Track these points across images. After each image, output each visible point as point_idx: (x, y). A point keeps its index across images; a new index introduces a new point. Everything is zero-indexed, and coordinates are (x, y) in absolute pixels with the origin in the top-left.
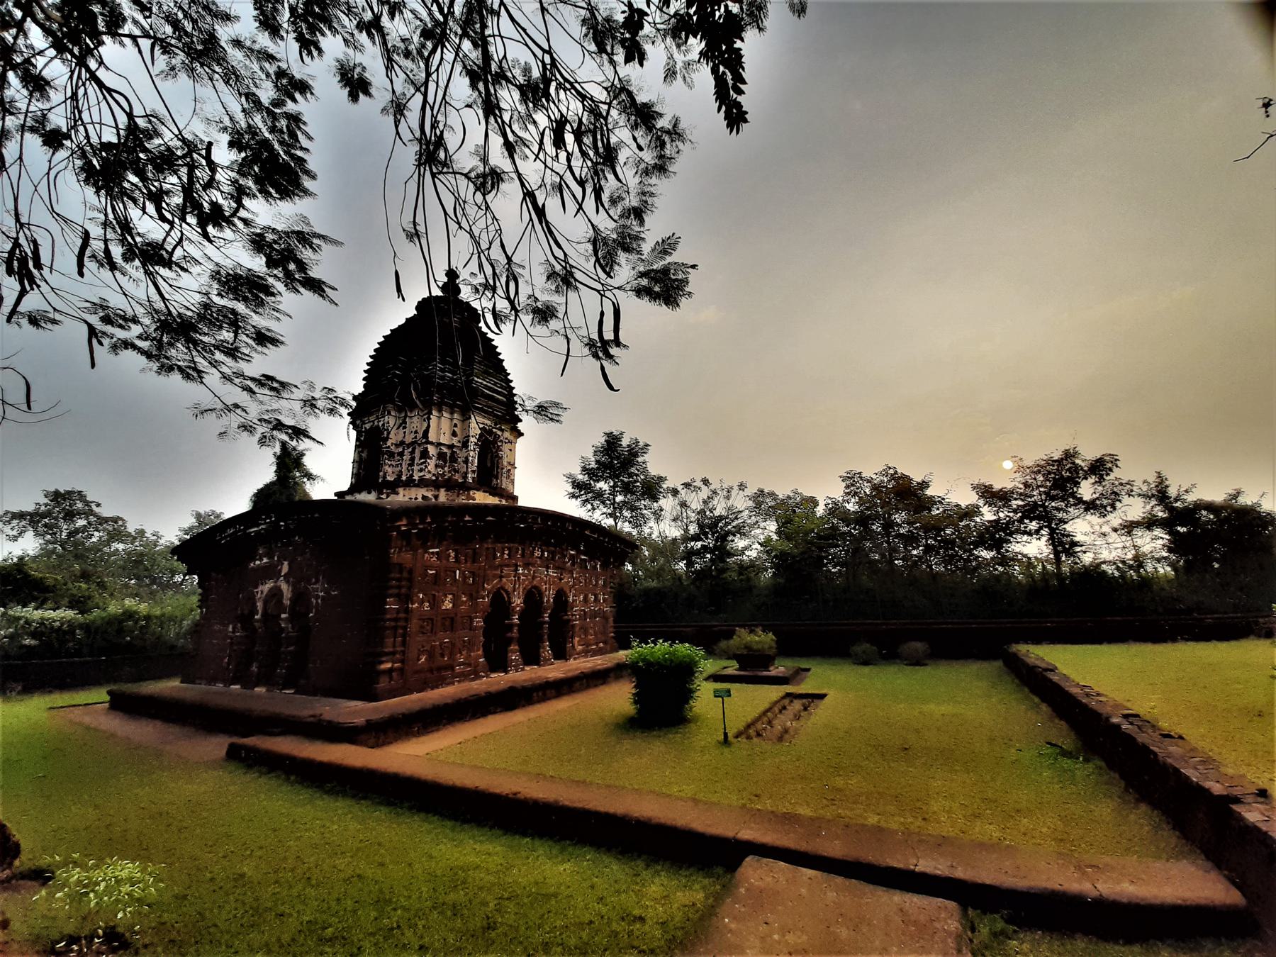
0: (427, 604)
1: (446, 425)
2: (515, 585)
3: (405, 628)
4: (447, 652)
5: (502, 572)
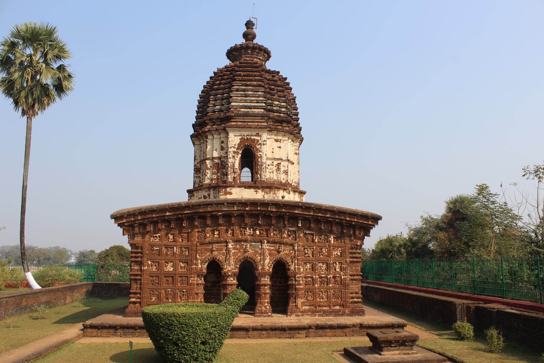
0: (155, 267)
1: (217, 144)
2: (226, 257)
3: (141, 280)
4: (170, 296)
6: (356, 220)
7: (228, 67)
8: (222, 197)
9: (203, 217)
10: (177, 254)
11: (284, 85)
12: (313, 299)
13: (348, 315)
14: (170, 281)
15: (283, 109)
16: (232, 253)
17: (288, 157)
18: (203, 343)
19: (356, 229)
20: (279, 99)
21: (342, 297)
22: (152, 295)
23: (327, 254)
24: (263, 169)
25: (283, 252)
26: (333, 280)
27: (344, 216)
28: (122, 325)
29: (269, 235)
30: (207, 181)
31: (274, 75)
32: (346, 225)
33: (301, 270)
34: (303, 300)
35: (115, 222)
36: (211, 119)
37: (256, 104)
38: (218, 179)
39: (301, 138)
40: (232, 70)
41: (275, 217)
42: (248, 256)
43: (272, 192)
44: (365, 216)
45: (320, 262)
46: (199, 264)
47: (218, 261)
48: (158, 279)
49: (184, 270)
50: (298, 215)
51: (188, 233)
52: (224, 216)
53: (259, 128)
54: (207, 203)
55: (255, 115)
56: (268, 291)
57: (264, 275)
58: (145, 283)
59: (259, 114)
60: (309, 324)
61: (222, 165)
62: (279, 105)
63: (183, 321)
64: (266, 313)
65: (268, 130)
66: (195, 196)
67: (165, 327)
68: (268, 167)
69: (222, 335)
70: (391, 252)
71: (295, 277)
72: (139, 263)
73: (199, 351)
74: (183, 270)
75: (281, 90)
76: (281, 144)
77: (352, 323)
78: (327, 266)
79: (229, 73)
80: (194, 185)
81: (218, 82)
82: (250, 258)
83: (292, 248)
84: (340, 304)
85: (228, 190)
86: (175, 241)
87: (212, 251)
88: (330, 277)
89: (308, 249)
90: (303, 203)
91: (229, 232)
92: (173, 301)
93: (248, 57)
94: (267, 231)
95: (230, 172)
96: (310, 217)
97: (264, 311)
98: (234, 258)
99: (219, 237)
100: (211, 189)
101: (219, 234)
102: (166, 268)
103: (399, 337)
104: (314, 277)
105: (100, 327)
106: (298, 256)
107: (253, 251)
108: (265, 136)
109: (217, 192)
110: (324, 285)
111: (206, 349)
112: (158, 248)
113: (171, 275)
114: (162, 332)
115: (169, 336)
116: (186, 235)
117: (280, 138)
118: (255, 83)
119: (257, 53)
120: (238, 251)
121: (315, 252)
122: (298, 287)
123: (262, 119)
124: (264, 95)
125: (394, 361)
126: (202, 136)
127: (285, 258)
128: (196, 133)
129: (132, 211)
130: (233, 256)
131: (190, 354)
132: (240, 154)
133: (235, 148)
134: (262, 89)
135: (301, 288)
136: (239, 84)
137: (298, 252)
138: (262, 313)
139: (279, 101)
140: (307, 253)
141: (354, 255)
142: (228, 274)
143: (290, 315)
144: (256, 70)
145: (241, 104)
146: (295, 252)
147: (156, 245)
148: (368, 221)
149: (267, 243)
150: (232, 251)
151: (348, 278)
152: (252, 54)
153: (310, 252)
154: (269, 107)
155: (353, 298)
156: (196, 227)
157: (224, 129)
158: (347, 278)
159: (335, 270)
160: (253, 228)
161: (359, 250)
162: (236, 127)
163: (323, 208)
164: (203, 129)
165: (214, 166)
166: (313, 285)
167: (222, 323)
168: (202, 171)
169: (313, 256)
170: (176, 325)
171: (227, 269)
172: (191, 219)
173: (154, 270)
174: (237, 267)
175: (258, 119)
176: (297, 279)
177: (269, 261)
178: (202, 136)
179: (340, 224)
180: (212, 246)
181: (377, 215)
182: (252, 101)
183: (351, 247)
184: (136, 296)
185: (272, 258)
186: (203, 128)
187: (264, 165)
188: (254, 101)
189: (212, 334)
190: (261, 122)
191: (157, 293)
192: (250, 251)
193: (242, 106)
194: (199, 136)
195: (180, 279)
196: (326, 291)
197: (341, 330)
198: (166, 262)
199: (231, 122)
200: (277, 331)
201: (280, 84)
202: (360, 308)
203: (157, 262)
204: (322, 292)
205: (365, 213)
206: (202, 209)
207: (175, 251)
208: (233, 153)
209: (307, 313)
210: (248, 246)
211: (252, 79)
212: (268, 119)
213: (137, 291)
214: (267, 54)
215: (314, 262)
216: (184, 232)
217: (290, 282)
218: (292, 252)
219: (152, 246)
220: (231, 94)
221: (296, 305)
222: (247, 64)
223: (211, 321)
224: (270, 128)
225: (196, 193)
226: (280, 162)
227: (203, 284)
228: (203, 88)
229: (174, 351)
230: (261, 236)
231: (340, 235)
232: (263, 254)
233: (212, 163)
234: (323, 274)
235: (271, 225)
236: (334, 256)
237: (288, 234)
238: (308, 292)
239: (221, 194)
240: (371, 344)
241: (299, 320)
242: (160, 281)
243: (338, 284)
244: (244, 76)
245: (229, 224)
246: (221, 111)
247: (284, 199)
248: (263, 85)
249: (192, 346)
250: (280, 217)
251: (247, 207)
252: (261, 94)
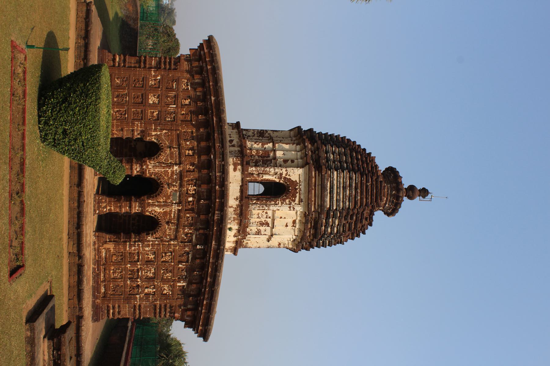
0: (153, 83)
1: (292, 155)
2: (164, 163)
3: (140, 67)
5: (174, 148)
6: (203, 311)
7: (376, 169)
8: (231, 160)
9: (209, 137)
10: (168, 108)
11: (356, 231)
12: (113, 262)
13: (94, 302)
14: (137, 100)
15: (329, 230)
16: (168, 169)
17: (275, 234)
18: (65, 132)
19: (193, 312)
20: (341, 224)
21: (114, 295)
22: (122, 79)
23: (165, 278)
24: (262, 207)
25: (168, 228)
26: (135, 285)
27: (208, 298)
28: (89, 44)
29: (187, 212)
30: (249, 144)
31: (368, 220)
32: (197, 300)
33: (147, 248)
34: (112, 250)
35: (205, 40)
36: (318, 149)
37: (335, 199)
38: (251, 156)
39: (298, 250)
40: (373, 173)
41: (208, 219)
42: (164, 188)
43: (236, 216)
44: (208, 322)
45: (156, 270)
46: (156, 133)
47: (158, 153)
48: (140, 87)
49: (150, 116)
50: (209, 245)
51: (191, 121)
52: (210, 161)
53: (308, 203)
54: (224, 142)
55: (322, 198)
56: (123, 210)
57: (142, 206)
58: (136, 72)
59: (324, 203)
60: (84, 256)
61: (267, 161)
62: (335, 225)
63: (90, 109)
64: (98, 208)
65: (306, 213)
66: (232, 131)
67: (84, 88)
68: (264, 212)
69: (74, 154)
70: (167, 356)
71: (138, 241)
72: (159, 66)
73: (56, 127)
74: (149, 114)
75: (351, 227)
76: (290, 227)
77: (84, 307)
78: (151, 278)
79: (370, 169)
80: (245, 130)
81: (359, 157)
82: (162, 190)
83: (172, 238)
84: (107, 293)
85: (239, 167)
86: (183, 106)
87: (170, 147)
88: (138, 282)
89: (170, 257)
90: (223, 250)
91: (191, 167)
92: (115, 103)
93: (388, 191)
94: (192, 210)
95: (259, 169)
96: (207, 259)
98: (162, 172)
99: (186, 155)
100: (240, 148)
101: (189, 155)
102: (152, 96)
103: (65, 359)
104: (138, 263)
105: (87, 20)
106: (162, 245)
107: (169, 194)
108: (299, 209)
109: (237, 155)
110: (130, 274)
111: (58, 135)
112: (174, 87)
113: (144, 101)
114: (78, 85)
115: (74, 93)
116: (189, 119)
117: (297, 226)
118: (359, 198)
119: (393, 201)
120: (169, 176)
121: (167, 264)
122: (128, 245)
123: (318, 206)
124: (345, 208)
125: (36, 354)
126: (300, 138)
127: (160, 230)
128: (303, 132)
129: (216, 59)
130: (164, 171)
131: (52, 116)
132: (280, 181)
133: (286, 175)
134: (352, 205)
135: (126, 248)
136: (357, 180)
137: (168, 244)
138: (98, 203)
139: (338, 225)
140: (166, 255)
141: (163, 310)
142: (144, 165)
143: (95, 235)
144: (373, 199)
145: (335, 182)
146: (168, 241)
147: (178, 85)
148: (202, 326)
149: (179, 210)
150: (170, 170)
151: (137, 302)
152: (391, 195)
153: (167, 258)
154: (332, 213)
155: (114, 308)
156: (198, 130)
157: (307, 163)
158: (137, 301)
159: (146, 288)
160: (195, 193)
161: (169, 315)
162: (309, 177)
163: (217, 274)
164: (307, 140)
165: (266, 151)
166: (129, 262)
167: (87, 153)
168: (261, 138)
169: (163, 262)
170: (86, 100)
171: (149, 164)
172: (207, 124)
173: (150, 83)
174: (151, 175)
175: (318, 201)
176: (137, 243)
177: (157, 212)
178: (300, 138)
179: (199, 293)
180: (176, 148)
181: (209, 336)
182: (339, 195)
183: (173, 306)
184: (122, 62)
185: (161, 215)
186: (309, 141)
187: (267, 208)
188: (339, 197)
189: (75, 141)
190: (315, 204)
191: (124, 85)
192: (170, 191)
193: (333, 183)
194: (299, 136)
195: (140, 112)
196: (122, 277)
197: (76, 293)
198: (159, 96)
199: (315, 171)
200: (77, 219)
201: (358, 227)
202: (102, 317)
203: (159, 86)
204: (121, 272)
205: (212, 321)
206: (218, 136)
207: (171, 106)
208: (280, 173)
209: (98, 254)
210: (175, 189)
211: (363, 195)
212: (318, 212)
213: (127, 63)
214: (391, 212)
215: (156, 263)
216: (193, 116)
217: (133, 236)
218: (168, 237)
219: (178, 81)
220: (347, 171)
221: (106, 242)
222: (380, 189)
223: (89, 140)
224: (309, 215)
225: (236, 132)
226: (270, 225)
227: (133, 136)
228: (352, 140)
229: (57, 98)
230: (186, 203)
231: (187, 293)
232: (166, 204)
233: (269, 149)
234: (142, 273)
235: (199, 214)
236: (162, 286)
237: (189, 233)
238: (121, 256)
239: (235, 159)
240: (58, 326)
241: (90, 245)
242: (138, 88)
243: (130, 291)
244: (367, 186)
245: (199, 167)
246: (328, 160)
247: (228, 231)
248: (357, 207)
249: (62, 119)
250: (208, 224)
251: (219, 187)
252: (346, 205)
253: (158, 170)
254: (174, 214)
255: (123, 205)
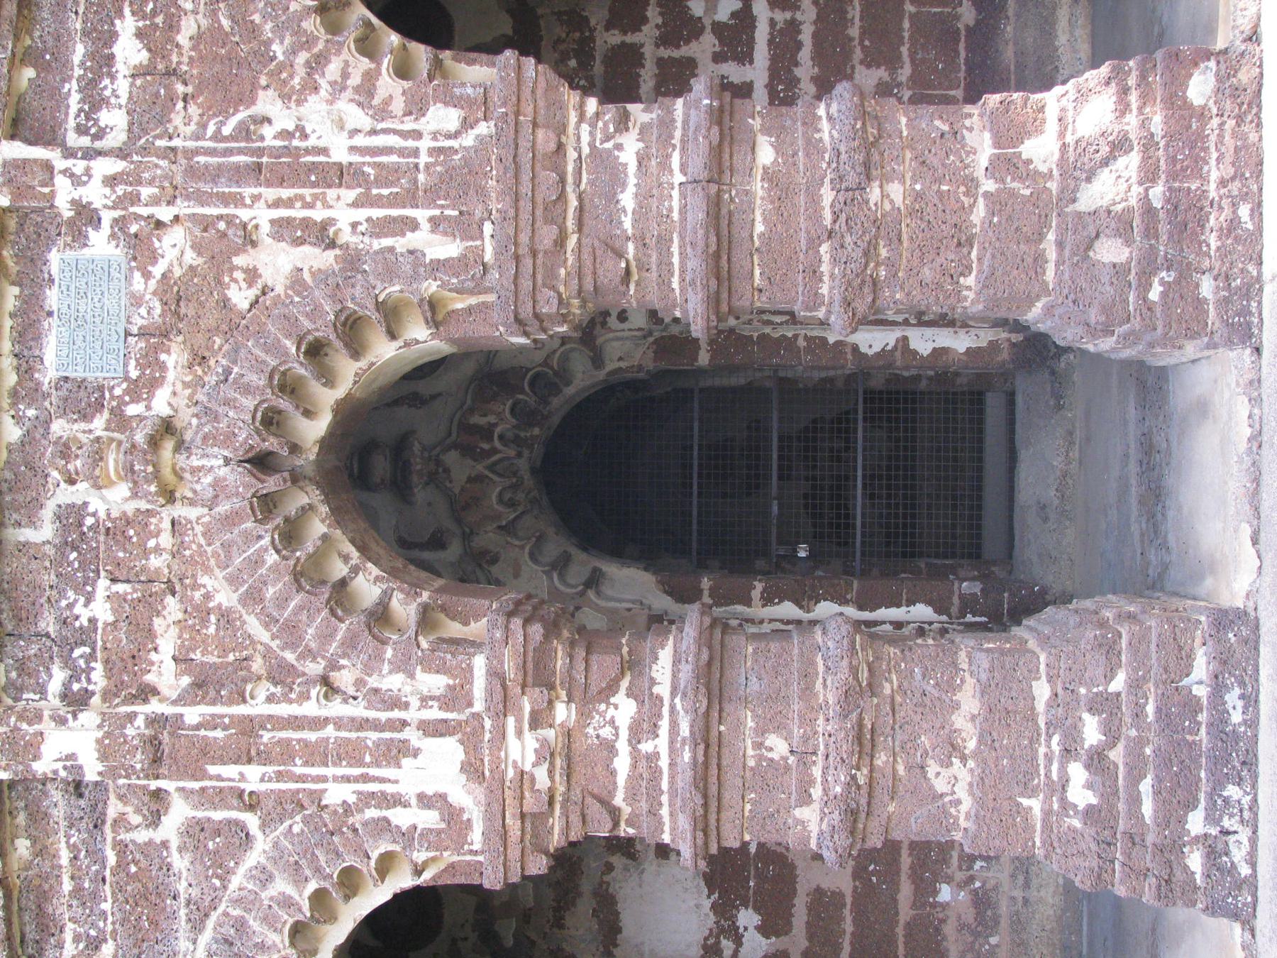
2: (252, 803)
16: (193, 714)
64: (1196, 143)
97: (1149, 175)
98: (282, 675)
150: (155, 707)
253: (336, 708)
254: (102, 62)
255: (827, 195)
